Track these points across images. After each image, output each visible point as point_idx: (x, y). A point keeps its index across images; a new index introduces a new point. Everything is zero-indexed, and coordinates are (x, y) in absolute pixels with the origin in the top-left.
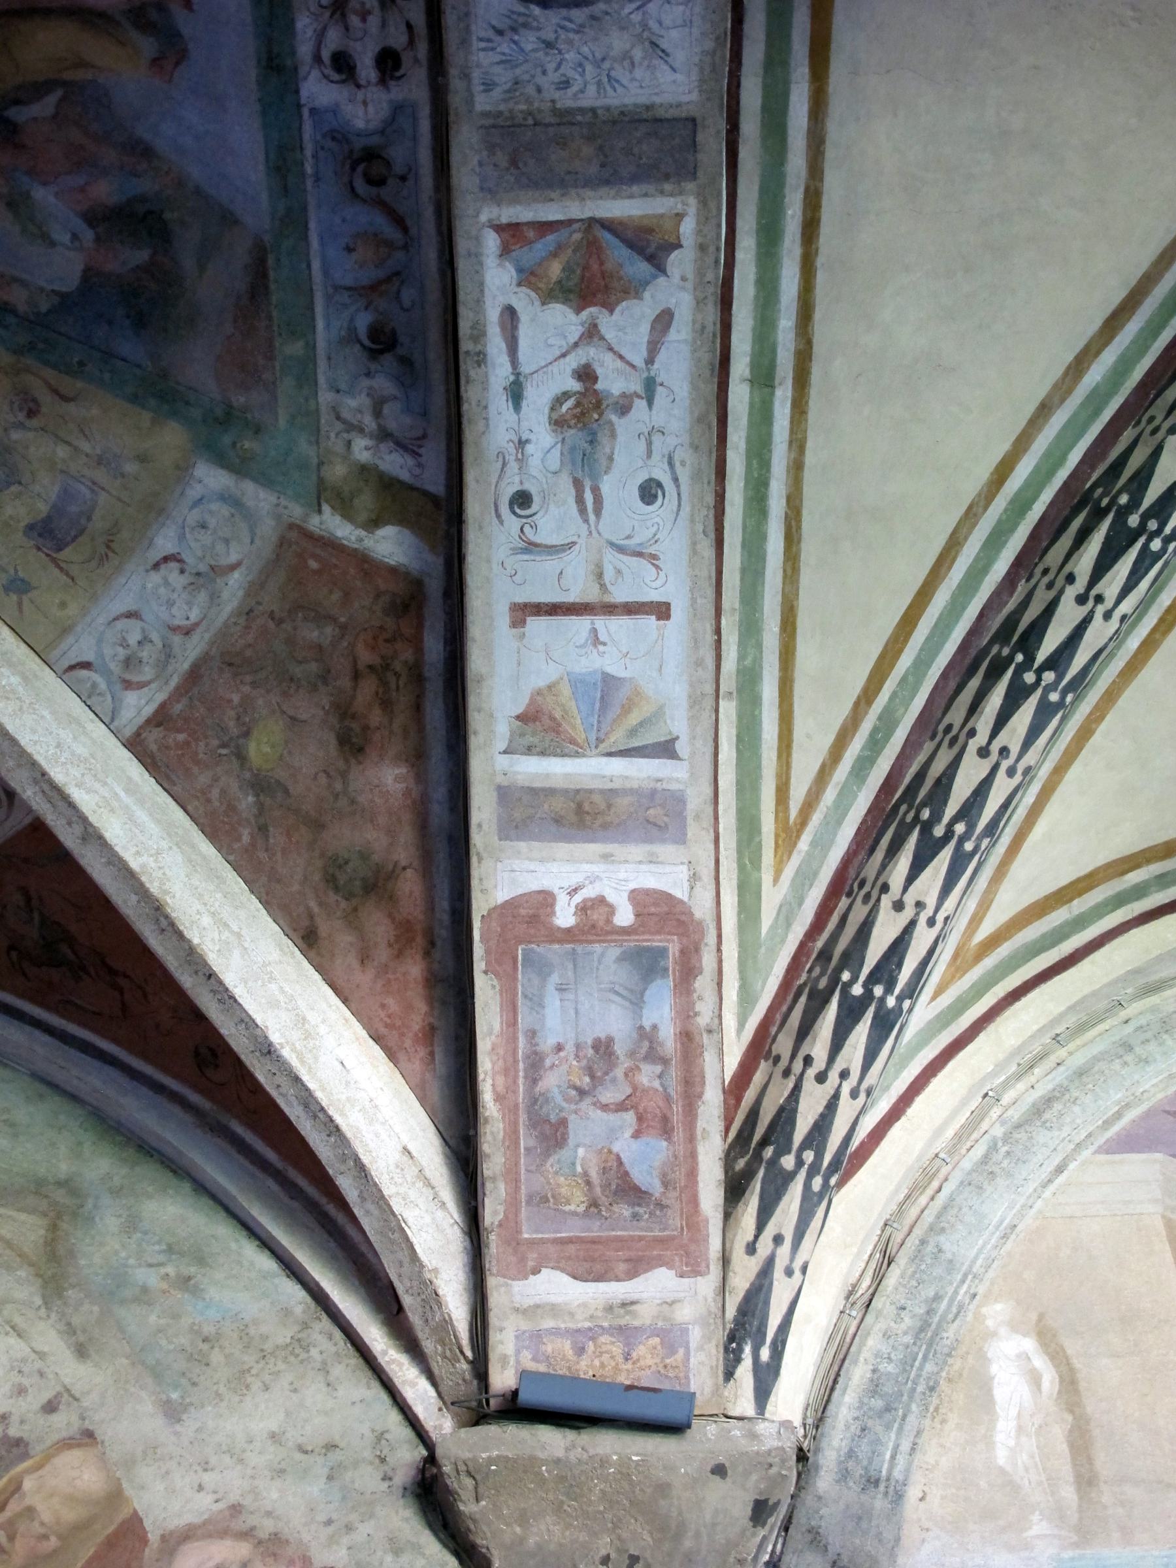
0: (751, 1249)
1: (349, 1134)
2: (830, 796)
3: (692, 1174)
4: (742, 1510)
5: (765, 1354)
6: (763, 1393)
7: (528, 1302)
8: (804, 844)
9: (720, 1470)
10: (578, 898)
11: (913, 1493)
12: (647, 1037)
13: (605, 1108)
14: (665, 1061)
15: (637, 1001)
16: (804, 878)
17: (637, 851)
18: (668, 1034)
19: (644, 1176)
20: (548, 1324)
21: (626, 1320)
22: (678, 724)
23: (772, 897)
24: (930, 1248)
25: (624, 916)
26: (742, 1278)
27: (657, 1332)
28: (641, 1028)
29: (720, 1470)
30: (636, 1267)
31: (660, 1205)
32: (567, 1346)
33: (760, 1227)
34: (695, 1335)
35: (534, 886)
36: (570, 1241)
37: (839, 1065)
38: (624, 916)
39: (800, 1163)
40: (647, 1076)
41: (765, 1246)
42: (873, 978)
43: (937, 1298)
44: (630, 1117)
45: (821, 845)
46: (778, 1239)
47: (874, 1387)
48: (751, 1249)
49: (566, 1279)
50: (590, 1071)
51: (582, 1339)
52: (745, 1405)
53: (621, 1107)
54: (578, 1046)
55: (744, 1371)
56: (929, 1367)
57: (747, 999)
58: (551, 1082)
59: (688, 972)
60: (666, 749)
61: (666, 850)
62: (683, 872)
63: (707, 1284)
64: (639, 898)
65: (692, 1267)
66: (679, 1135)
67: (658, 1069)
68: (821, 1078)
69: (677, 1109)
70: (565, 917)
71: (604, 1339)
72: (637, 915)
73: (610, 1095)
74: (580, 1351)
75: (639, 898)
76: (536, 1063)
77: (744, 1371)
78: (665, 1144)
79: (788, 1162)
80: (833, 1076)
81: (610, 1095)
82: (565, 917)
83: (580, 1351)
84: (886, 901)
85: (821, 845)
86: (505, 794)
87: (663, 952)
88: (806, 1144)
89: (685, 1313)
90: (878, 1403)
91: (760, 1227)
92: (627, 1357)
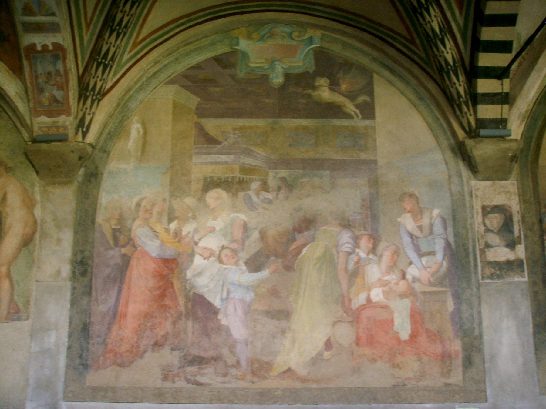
0: (81, 110)
1: (5, 90)
2: (95, 17)
3: (68, 97)
4: (77, 158)
5: (84, 130)
6: (84, 136)
7: (39, 122)
8: (91, 27)
9: (72, 152)
10: (41, 44)
11: (111, 154)
12: (58, 72)
13: (51, 85)
14: (61, 76)
15: (55, 64)
16: (92, 34)
17: (51, 35)
18: (62, 70)
19: (59, 98)
20: (44, 125)
21: (57, 125)
22: (55, 9)
23: (86, 38)
24: (126, 105)
25: (51, 48)
26: (80, 116)
27: (63, 127)
28: (57, 70)
29: (72, 152)
30: (59, 114)
31: (62, 103)
32: (46, 129)
33: (83, 106)
34: (69, 127)
35: (32, 42)
36: (46, 110)
37: (97, 75)
38: (51, 48)
39: (90, 94)
40: (58, 79)
41: (84, 110)
42: (103, 58)
43: (125, 116)
44: (55, 87)
45: (95, 27)
46: (87, 109)
47: (109, 134)
48: (81, 110)
49: (45, 117)
50: (47, 78)
51: (49, 128)
52: (80, 139)
53: (54, 85)
54: (45, 74)
55: (80, 133)
56: (120, 130)
57: (83, 59)
58: (40, 80)
59: (64, 58)
60: (53, 14)
61: (57, 35)
62: (61, 39)
63: (71, 118)
64: (53, 44)
65: (69, 114)
66: (65, 90)
67: (61, 77)
68: (94, 78)
69: (65, 85)
70: (39, 48)
71: (54, 128)
72: (53, 47)
73: (51, 83)
74: (49, 130)
75: (53, 44)
76: (37, 77)
77: (80, 133)
78: (63, 92)
79: (88, 94)
80: (96, 77)
81: (51, 83)
82: (39, 48)
83: (49, 130)
84: (105, 42)
85: (95, 27)
86: (24, 24)
87: (59, 55)
88: (92, 90)
89: (67, 123)
90: (109, 137)
91: (83, 106)
92: (57, 131)
